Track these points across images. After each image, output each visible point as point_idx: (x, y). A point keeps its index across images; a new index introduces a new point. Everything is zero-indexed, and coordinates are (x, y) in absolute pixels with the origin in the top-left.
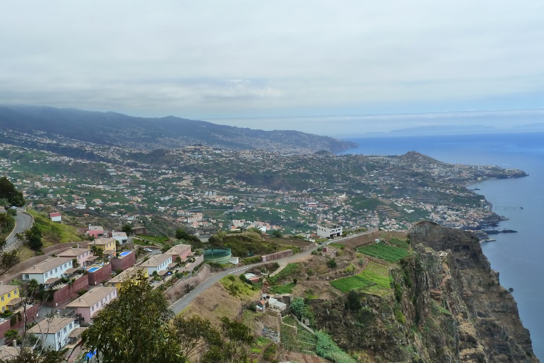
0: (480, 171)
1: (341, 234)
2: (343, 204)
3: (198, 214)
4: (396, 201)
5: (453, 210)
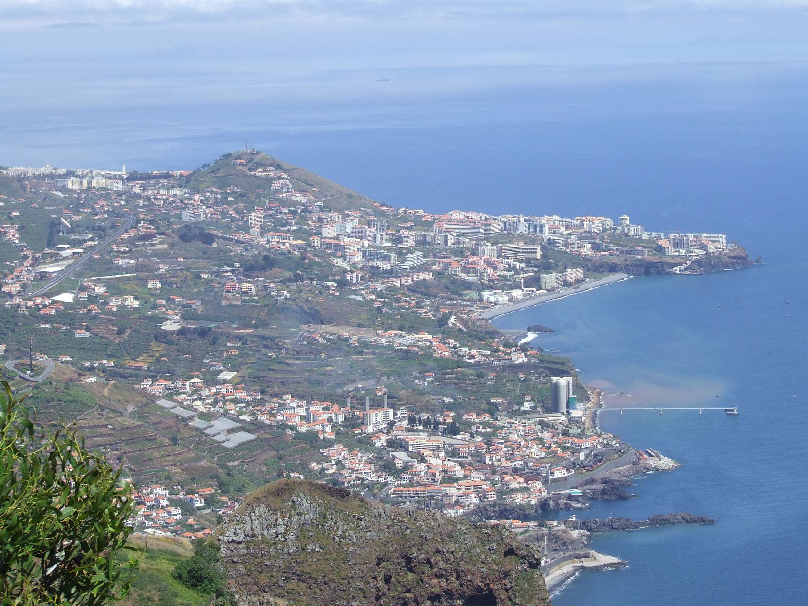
4: (170, 397)
5: (431, 426)
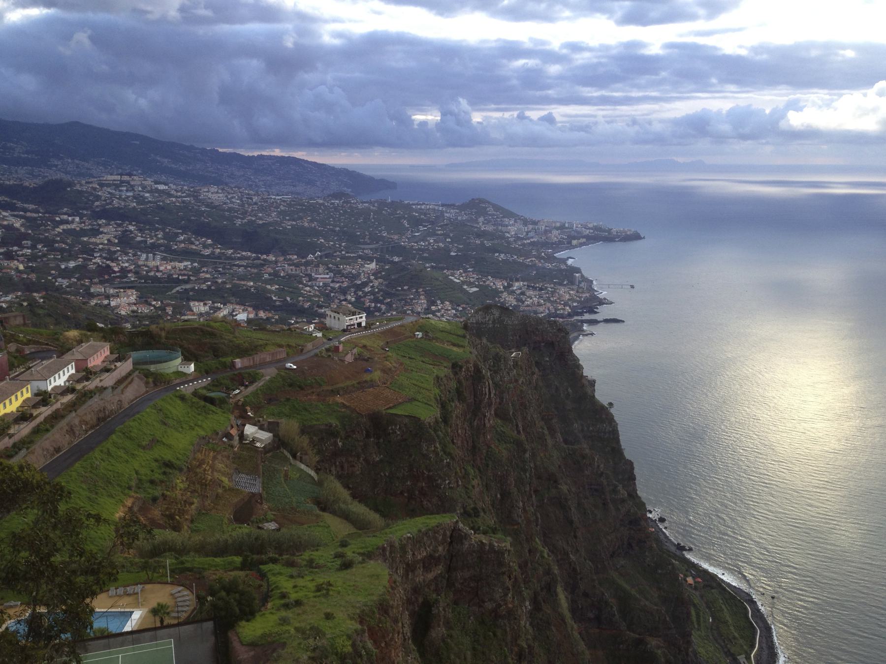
0: (576, 231)
1: (363, 324)
2: (372, 277)
3: (129, 292)
4: (452, 276)
5: (534, 288)
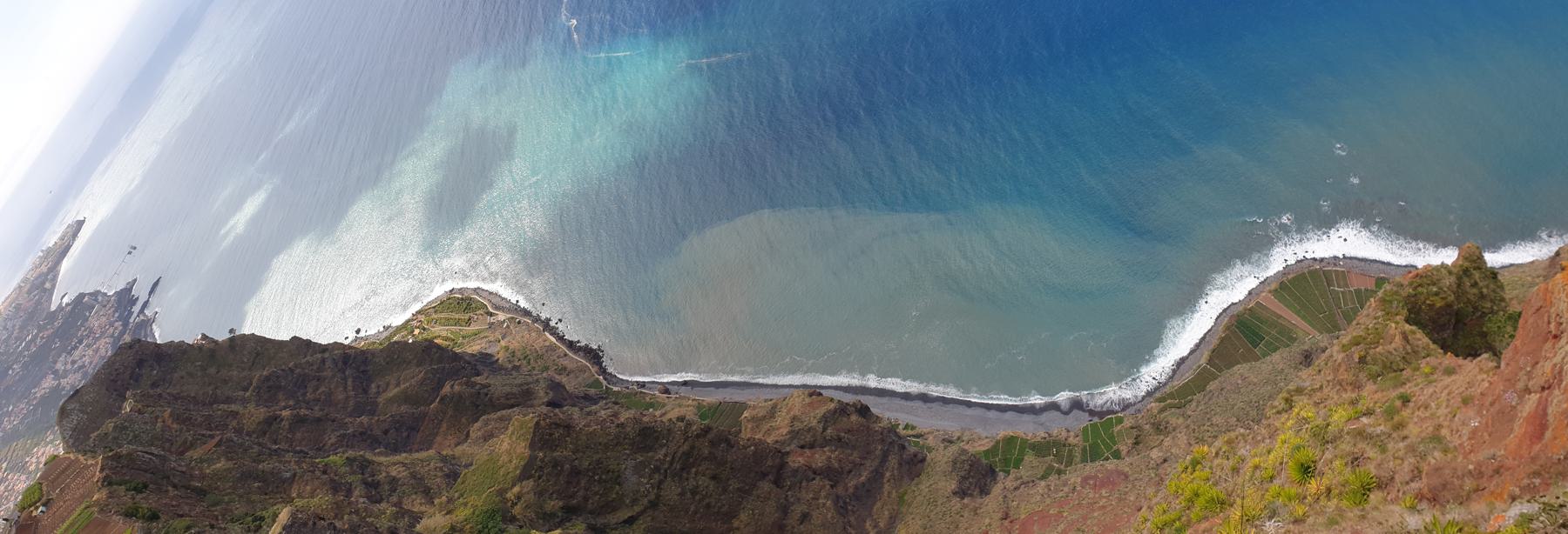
5: (76, 348)
